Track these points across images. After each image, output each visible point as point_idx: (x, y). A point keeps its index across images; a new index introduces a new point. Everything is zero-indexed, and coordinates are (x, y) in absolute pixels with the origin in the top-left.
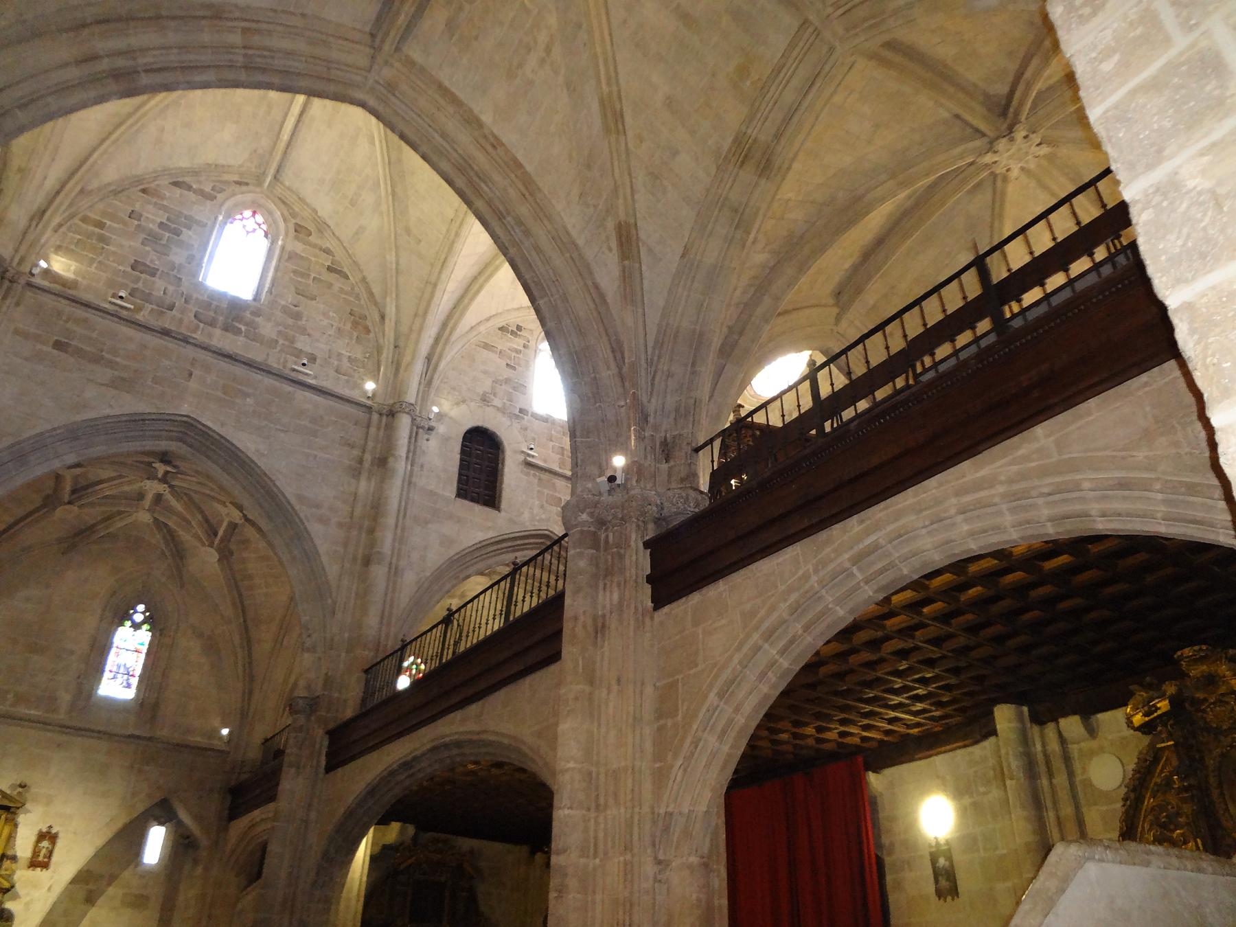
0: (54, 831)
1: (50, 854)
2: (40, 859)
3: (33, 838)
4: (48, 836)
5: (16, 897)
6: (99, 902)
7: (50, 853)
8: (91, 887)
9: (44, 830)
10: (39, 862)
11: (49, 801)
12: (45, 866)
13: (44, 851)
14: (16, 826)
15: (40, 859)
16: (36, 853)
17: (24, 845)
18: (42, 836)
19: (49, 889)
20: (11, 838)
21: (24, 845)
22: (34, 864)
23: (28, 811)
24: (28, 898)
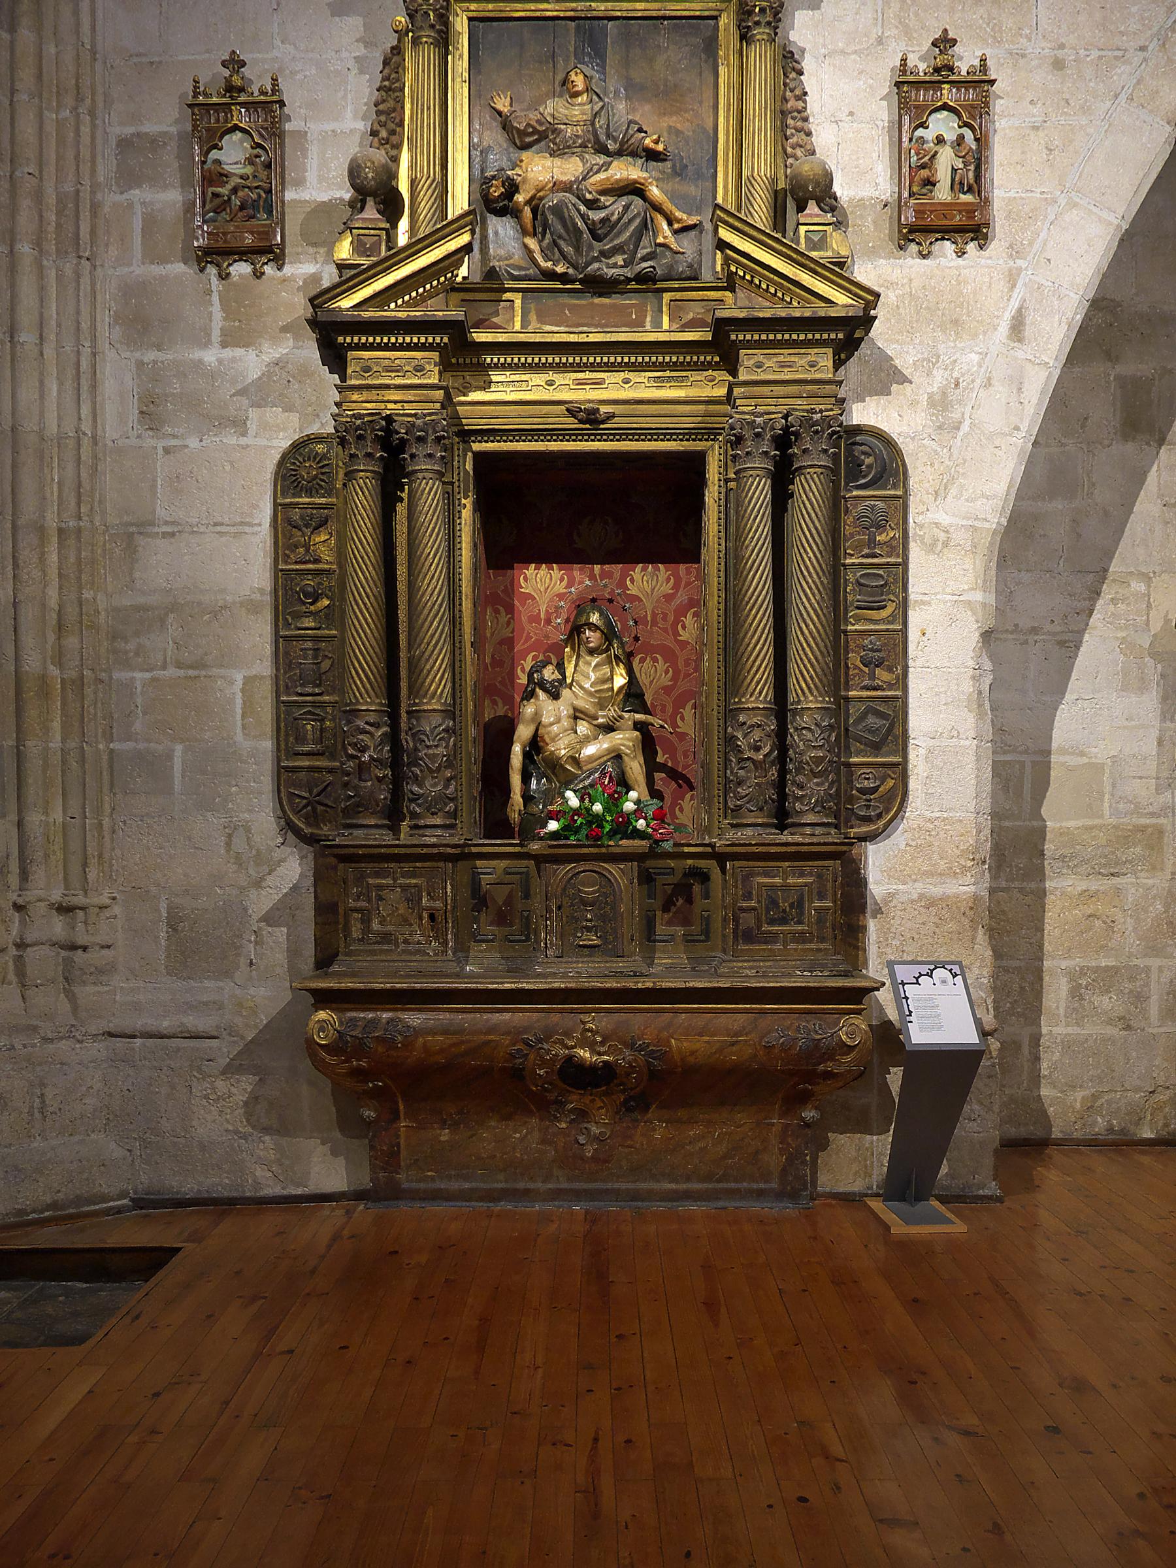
0: (965, 60)
1: (974, 176)
3: (881, 112)
4: (939, 89)
5: (887, 378)
7: (977, 160)
8: (1127, 368)
9: (921, 66)
12: (971, 229)
13: (946, 160)
14: (788, 62)
15: (942, 193)
16: (917, 175)
17: (853, 140)
18: (914, 94)
19: (1017, 328)
20: (789, 115)
21: (853, 140)
24: (939, 378)
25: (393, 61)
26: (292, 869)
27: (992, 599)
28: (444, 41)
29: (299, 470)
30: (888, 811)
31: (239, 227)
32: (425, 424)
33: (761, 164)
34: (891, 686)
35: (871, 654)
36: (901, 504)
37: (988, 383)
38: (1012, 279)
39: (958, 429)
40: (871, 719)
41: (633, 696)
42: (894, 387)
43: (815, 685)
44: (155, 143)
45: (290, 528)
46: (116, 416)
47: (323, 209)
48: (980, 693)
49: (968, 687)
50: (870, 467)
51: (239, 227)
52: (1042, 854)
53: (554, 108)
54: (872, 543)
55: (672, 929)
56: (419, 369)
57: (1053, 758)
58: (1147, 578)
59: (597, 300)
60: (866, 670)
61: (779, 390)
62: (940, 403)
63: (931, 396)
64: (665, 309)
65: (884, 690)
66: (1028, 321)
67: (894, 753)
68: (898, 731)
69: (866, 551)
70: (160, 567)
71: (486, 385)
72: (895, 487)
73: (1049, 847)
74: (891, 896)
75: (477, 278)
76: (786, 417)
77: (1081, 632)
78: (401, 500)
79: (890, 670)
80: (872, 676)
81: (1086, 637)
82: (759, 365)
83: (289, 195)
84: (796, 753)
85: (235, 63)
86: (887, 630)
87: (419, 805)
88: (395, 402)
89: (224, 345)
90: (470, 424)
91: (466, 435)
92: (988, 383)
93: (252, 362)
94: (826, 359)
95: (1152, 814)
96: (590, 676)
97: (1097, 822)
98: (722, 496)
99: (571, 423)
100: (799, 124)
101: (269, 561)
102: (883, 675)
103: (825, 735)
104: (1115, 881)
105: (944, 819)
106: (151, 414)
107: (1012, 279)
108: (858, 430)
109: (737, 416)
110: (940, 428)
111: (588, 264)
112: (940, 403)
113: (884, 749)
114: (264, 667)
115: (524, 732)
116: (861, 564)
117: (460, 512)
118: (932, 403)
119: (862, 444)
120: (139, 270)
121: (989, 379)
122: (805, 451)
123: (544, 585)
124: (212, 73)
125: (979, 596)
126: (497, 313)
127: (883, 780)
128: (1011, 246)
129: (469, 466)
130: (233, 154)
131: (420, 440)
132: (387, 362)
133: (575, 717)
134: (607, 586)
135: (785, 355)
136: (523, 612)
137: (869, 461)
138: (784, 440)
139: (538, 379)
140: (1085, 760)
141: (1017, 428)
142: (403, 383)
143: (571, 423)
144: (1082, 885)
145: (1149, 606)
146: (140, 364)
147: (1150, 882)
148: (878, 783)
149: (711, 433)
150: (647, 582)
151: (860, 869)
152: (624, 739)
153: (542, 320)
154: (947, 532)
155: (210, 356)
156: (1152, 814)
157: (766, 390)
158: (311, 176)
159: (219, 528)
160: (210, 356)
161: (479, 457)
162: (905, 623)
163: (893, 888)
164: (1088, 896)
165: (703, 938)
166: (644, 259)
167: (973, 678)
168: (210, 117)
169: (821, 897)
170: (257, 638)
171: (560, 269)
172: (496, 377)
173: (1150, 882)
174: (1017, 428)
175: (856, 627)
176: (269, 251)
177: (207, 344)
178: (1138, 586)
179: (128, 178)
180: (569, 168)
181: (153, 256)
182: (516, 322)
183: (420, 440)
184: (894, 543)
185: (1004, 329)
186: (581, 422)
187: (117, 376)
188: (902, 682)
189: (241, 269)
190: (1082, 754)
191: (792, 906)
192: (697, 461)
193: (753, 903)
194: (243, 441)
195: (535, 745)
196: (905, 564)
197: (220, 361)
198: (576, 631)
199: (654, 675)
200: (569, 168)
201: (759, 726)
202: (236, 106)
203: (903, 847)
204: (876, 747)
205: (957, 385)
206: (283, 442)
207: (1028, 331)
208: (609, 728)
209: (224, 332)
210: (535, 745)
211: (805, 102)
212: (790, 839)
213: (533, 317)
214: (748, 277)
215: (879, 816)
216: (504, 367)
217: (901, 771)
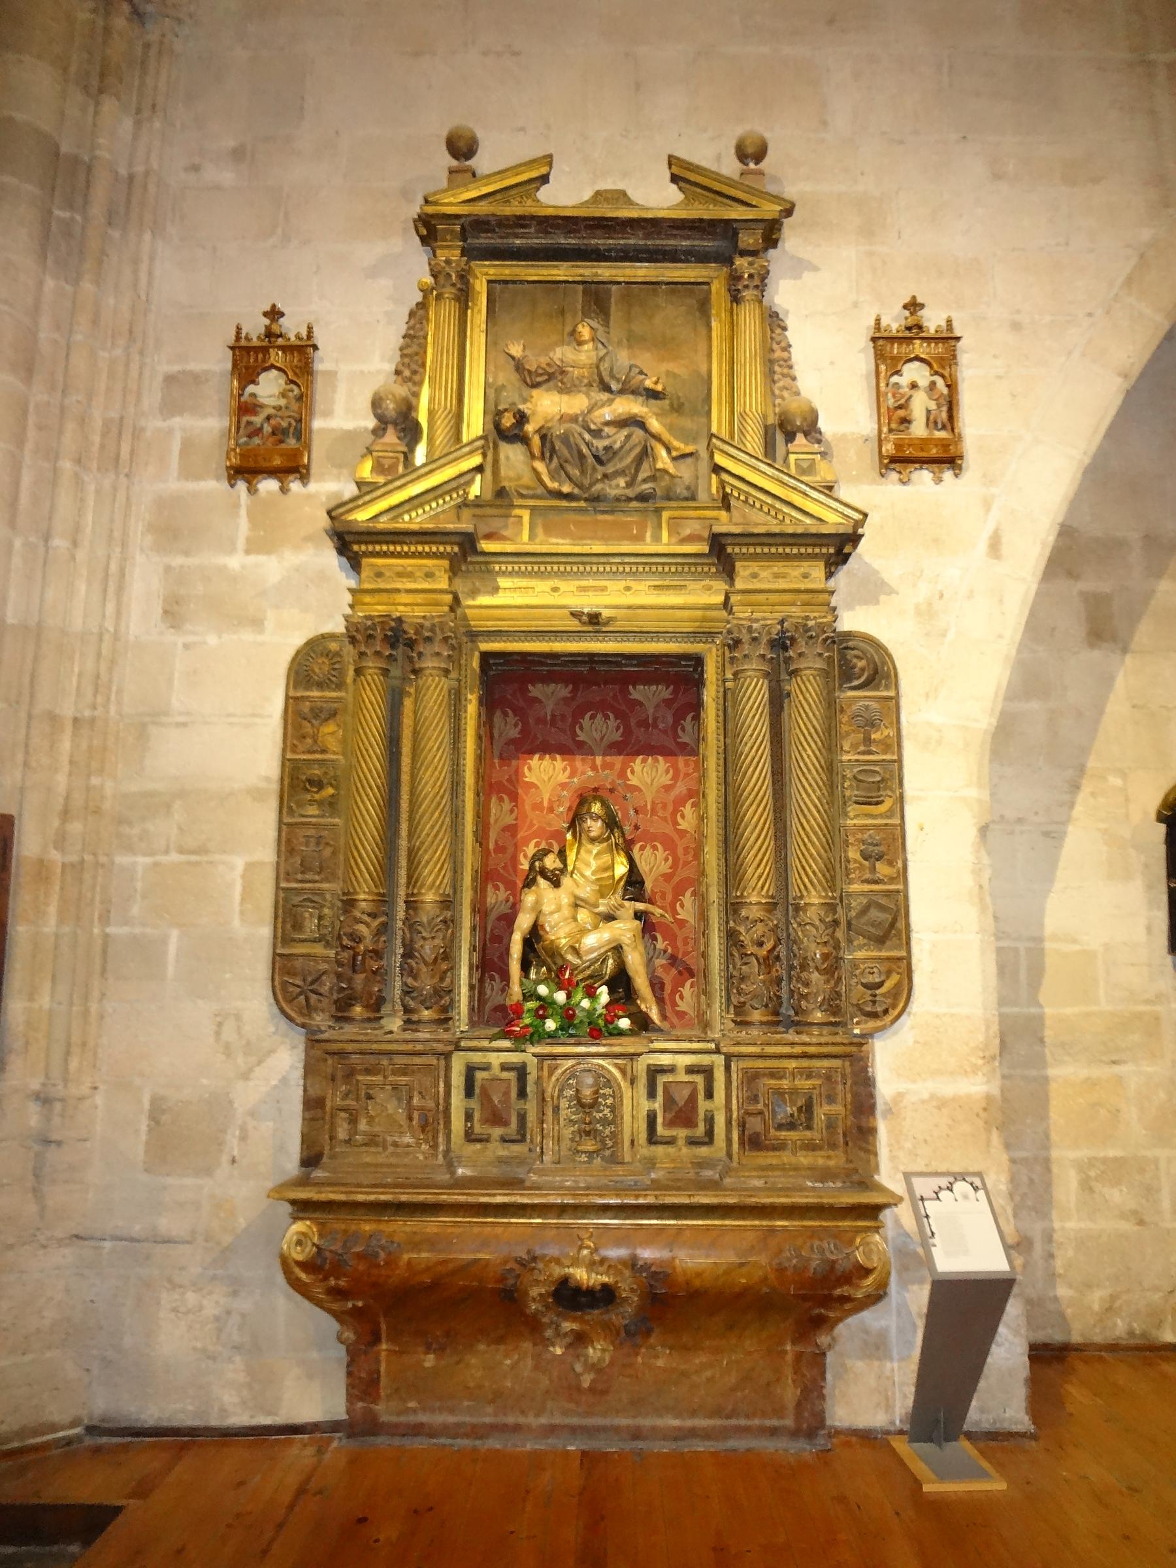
0: (933, 320)
2: (919, 429)
4: (910, 343)
5: (874, 590)
6: (1144, 633)
10: (924, 449)
11: (870, 222)
12: (947, 459)
13: (920, 405)
14: (773, 321)
15: (919, 429)
18: (890, 348)
19: (995, 546)
20: (776, 363)
22: (900, 460)
23: (800, 267)
25: (419, 313)
26: (285, 1061)
27: (986, 796)
28: (464, 297)
29: (312, 668)
30: (894, 1006)
31: (268, 452)
32: (434, 625)
33: (753, 401)
34: (892, 880)
35: (871, 848)
36: (893, 705)
37: (971, 595)
38: (987, 505)
39: (944, 635)
40: (874, 914)
41: (634, 884)
42: (882, 598)
43: (819, 881)
44: (197, 379)
45: (300, 720)
46: (141, 618)
47: (349, 437)
48: (981, 887)
49: (969, 881)
50: (863, 670)
51: (268, 452)
52: (1042, 1041)
53: (562, 354)
54: (867, 741)
55: (673, 1132)
56: (429, 575)
57: (1048, 945)
58: (1124, 775)
59: (601, 517)
60: (866, 863)
61: (774, 598)
62: (926, 613)
63: (917, 607)
64: (664, 525)
65: (885, 883)
66: (1004, 540)
67: (898, 947)
68: (901, 924)
69: (862, 748)
70: (173, 757)
71: (496, 590)
72: (887, 688)
73: (1048, 1034)
74: (900, 1095)
75: (489, 496)
76: (782, 622)
77: (1065, 823)
78: (409, 694)
79: (891, 863)
80: (873, 869)
81: (1070, 828)
82: (754, 576)
83: (317, 424)
84: (800, 949)
85: (274, 314)
86: (886, 825)
87: (413, 998)
88: (405, 605)
89: (248, 552)
90: (476, 625)
91: (474, 636)
92: (971, 595)
93: (273, 568)
94: (817, 571)
95: (1148, 1002)
96: (592, 864)
97: (1094, 1008)
98: (721, 695)
99: (574, 625)
100: (786, 371)
101: (277, 751)
102: (882, 869)
103: (830, 931)
104: (1117, 1069)
105: (952, 1015)
106: (173, 613)
107: (987, 505)
108: (849, 635)
109: (735, 622)
110: (927, 635)
111: (592, 485)
112: (926, 613)
113: (888, 943)
114: (267, 854)
115: (524, 922)
116: (857, 761)
117: (465, 706)
118: (918, 612)
119: (853, 649)
120: (174, 485)
121: (972, 591)
122: (800, 655)
123: (547, 775)
124: (255, 327)
125: (973, 793)
126: (506, 526)
127: (889, 973)
128: (984, 476)
129: (476, 664)
130: (269, 388)
131: (428, 639)
132: (400, 569)
133: (577, 909)
134: (608, 778)
135: (778, 567)
136: (527, 802)
137: (861, 664)
138: (781, 643)
139: (543, 586)
140: (1077, 947)
141: (1000, 636)
142: (415, 588)
143: (574, 625)
144: (1084, 1073)
145: (1127, 800)
146: (168, 569)
147: (1149, 1069)
148: (883, 978)
149: (710, 635)
150: (647, 775)
151: (867, 1066)
152: (625, 929)
153: (548, 531)
154: (940, 731)
155: (235, 562)
156: (1148, 1002)
157: (761, 597)
158: (339, 406)
159: (231, 720)
160: (235, 562)
161: (485, 656)
162: (903, 818)
163: (902, 1087)
164: (1091, 1084)
165: (706, 1140)
166: (645, 481)
167: (973, 872)
168: (248, 359)
169: (831, 1099)
170: (260, 829)
171: (566, 489)
172: (503, 582)
173: (1149, 1069)
174: (1000, 636)
175: (855, 821)
176: (294, 469)
177: (232, 550)
178: (1115, 781)
179: (170, 408)
180: (577, 403)
181: (187, 473)
182: (523, 533)
183: (428, 639)
184: (889, 741)
185: (983, 546)
186: (584, 623)
187: (146, 577)
188: (902, 875)
189: (268, 486)
190: (1075, 941)
191: (800, 1109)
192: (698, 661)
193: (760, 1106)
194: (260, 638)
195: (534, 936)
196: (900, 761)
197: (243, 567)
198: (576, 821)
199: (653, 863)
200: (577, 403)
201: (761, 921)
202: (273, 351)
203: (910, 1042)
204: (881, 941)
205: (941, 596)
206: (298, 640)
207: (1005, 549)
208: (610, 918)
209: (248, 540)
210: (534, 936)
211: (789, 353)
212: (797, 1039)
213: (540, 531)
214: (742, 498)
215: (886, 1012)
216: (511, 574)
217: (904, 966)
